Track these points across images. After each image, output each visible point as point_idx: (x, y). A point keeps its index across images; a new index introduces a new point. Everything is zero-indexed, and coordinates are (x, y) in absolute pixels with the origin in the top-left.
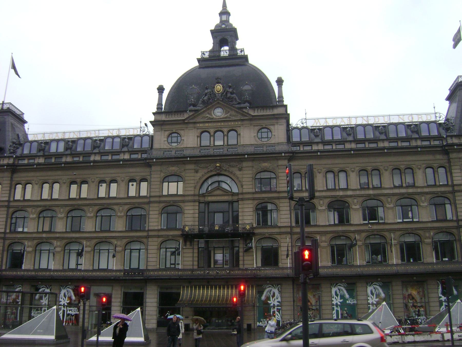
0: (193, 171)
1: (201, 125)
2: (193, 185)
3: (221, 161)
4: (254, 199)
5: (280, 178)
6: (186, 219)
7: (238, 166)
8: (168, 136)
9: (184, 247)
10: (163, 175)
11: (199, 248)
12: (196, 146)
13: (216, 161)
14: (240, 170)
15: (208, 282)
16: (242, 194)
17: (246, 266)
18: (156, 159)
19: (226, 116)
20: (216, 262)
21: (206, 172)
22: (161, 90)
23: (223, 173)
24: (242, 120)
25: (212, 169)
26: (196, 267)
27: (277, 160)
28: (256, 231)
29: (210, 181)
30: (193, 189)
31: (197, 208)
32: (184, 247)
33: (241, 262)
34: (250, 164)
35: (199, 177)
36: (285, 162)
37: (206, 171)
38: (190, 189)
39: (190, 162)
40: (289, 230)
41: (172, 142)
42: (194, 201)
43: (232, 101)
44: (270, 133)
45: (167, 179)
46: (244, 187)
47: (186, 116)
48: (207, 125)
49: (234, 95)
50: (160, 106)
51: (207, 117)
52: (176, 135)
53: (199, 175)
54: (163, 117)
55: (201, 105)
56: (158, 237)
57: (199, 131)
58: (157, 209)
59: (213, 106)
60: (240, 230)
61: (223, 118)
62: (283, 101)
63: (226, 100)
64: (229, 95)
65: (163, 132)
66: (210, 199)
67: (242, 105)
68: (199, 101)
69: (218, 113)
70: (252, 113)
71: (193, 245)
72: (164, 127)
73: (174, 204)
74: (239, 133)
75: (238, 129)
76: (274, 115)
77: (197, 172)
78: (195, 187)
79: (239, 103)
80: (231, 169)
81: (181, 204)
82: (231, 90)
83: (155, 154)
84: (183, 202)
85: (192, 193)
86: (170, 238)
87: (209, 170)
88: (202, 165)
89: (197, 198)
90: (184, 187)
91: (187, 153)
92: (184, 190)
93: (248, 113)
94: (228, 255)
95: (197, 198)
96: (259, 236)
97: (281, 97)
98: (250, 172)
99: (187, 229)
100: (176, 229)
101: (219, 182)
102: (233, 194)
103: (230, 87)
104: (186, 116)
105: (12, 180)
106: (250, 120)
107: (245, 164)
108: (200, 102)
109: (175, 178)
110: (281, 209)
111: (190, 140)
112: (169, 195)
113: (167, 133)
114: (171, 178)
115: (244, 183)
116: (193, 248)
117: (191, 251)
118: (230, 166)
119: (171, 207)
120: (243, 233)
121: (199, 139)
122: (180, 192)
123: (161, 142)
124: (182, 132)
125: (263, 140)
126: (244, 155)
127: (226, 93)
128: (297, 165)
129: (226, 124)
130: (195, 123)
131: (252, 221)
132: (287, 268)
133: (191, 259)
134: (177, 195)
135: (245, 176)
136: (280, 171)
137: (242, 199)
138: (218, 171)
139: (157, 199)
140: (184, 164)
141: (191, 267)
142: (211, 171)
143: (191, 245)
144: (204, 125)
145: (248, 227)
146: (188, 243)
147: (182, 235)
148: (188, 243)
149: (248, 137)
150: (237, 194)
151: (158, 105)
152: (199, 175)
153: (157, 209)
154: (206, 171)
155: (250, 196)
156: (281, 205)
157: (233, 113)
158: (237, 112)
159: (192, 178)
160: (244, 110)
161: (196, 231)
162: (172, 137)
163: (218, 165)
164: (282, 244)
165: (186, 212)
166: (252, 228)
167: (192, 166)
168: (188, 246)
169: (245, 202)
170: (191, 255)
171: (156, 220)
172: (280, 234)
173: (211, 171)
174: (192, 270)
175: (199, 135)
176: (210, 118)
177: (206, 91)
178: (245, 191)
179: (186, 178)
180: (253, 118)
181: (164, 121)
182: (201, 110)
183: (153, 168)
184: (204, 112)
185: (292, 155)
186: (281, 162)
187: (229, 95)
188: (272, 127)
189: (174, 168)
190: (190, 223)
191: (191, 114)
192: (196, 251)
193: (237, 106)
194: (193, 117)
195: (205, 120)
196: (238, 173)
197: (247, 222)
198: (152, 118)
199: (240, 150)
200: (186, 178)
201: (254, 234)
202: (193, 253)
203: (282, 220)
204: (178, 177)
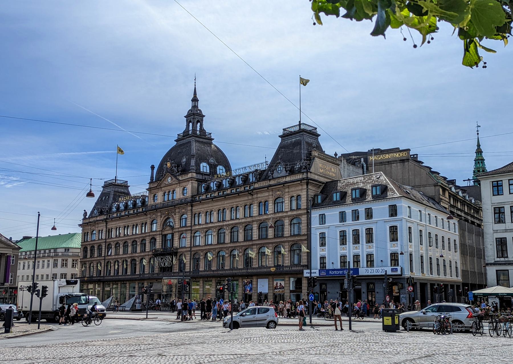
22: (153, 167)
53: (162, 219)
54: (152, 186)
63: (171, 172)
85: (159, 230)
91: (159, 206)
105: (106, 228)
106: (179, 183)
111: (160, 199)
130: (161, 188)
152: (162, 219)
155: (177, 230)
180: (180, 182)
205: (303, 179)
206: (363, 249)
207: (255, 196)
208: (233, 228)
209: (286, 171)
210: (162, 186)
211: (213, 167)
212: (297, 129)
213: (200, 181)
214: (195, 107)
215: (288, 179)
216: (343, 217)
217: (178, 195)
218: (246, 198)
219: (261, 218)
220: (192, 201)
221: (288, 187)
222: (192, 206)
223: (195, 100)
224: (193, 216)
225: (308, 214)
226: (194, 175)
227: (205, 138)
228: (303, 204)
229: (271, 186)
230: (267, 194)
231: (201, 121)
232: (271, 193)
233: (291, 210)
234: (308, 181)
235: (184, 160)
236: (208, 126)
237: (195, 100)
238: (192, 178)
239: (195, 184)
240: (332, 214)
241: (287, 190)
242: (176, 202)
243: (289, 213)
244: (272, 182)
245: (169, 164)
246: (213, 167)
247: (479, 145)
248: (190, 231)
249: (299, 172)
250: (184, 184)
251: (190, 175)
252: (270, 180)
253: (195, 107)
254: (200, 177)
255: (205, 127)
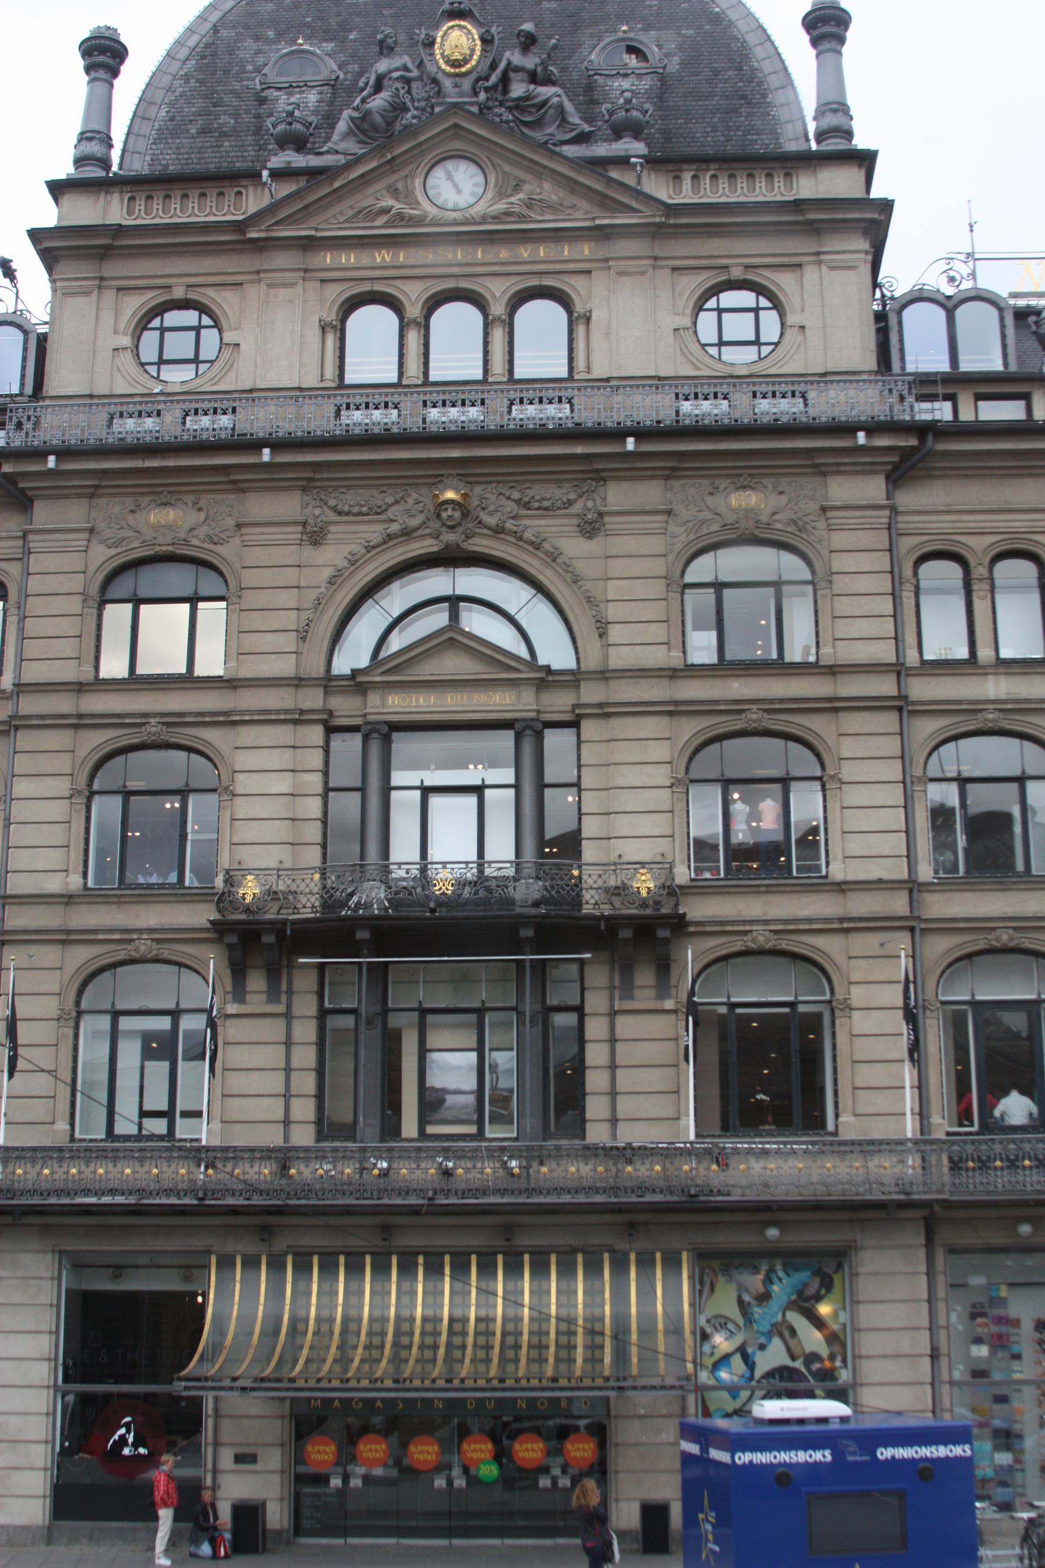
0: (294, 533)
1: (348, 258)
2: (290, 619)
3: (466, 470)
4: (676, 710)
5: (841, 584)
6: (248, 832)
7: (577, 508)
8: (142, 325)
9: (232, 1009)
10: (102, 556)
11: (323, 1014)
12: (311, 380)
13: (437, 471)
14: (590, 528)
15: (384, 1233)
16: (604, 675)
17: (630, 1134)
18: (64, 453)
19: (501, 206)
20: (431, 1103)
21: (376, 538)
22: (104, 54)
23: (481, 545)
24: (602, 234)
25: (414, 523)
26: (304, 1136)
27: (822, 472)
28: (696, 910)
29: (399, 596)
30: (288, 642)
31: (316, 759)
32: (232, 1009)
33: (595, 1107)
34: (650, 493)
35: (327, 573)
36: (873, 488)
37: (374, 532)
38: (269, 641)
39: (272, 479)
40: (898, 904)
41: (161, 362)
42: (298, 719)
43: (538, 124)
44: (770, 320)
45: (124, 585)
46: (616, 633)
47: (254, 201)
48: (383, 257)
49: (546, 91)
50: (95, 148)
51: (386, 211)
52: (190, 317)
54: (112, 211)
55: (353, 147)
56: (67, 938)
57: (336, 293)
58: (64, 763)
59: (421, 150)
60: (592, 903)
61: (484, 219)
62: (849, 134)
63: (503, 115)
64: (518, 89)
65: (110, 295)
66: (398, 704)
67: (601, 150)
68: (330, 120)
69: (456, 189)
71: (290, 992)
72: (114, 268)
73: (167, 736)
74: (579, 308)
75: (575, 286)
76: (798, 205)
77: (316, 537)
78: (303, 635)
79: (583, 138)
80: (534, 526)
81: (213, 736)
82: (530, 62)
83: (56, 426)
84: (228, 720)
85: (285, 667)
86: (143, 946)
87: (394, 528)
88: (351, 499)
89: (312, 699)
90: (234, 633)
91: (257, 420)
92: (234, 651)
93: (638, 194)
94: (505, 1060)
95: (312, 699)
96: (711, 942)
97: (834, 107)
98: (655, 544)
99: (250, 889)
100: (178, 893)
101: (454, 602)
102: (547, 679)
103: (528, 42)
104: (254, 201)
106: (655, 232)
107: (617, 495)
108: (342, 126)
109: (179, 578)
110: (847, 772)
111: (273, 347)
112: (136, 681)
113: (134, 305)
114: (150, 580)
115: (613, 612)
116: (288, 1016)
117: (275, 1029)
118: (527, 506)
120: (613, 923)
121: (331, 341)
122: (211, 662)
124: (225, 301)
125: (730, 354)
126: (619, 434)
127: (505, 80)
129: (504, 253)
130: (309, 244)
131: (664, 845)
132: (895, 1146)
133: (275, 1083)
134: (188, 681)
135: (617, 567)
136: (839, 539)
137: (605, 712)
138: (449, 537)
139: (63, 704)
140: (239, 488)
141: (273, 1137)
142: (407, 534)
143: (273, 993)
144: (365, 261)
145: (645, 883)
146: (257, 982)
147: (220, 929)
148: (257, 982)
149: (636, 335)
150: (573, 679)
151: (84, 137)
152: (331, 556)
153: (64, 763)
154: (374, 532)
156: (848, 748)
157: (548, 191)
158: (572, 186)
159: (290, 576)
160: (614, 174)
161: (308, 906)
162: (163, 330)
163: (450, 495)
164: (855, 990)
165: (243, 783)
166: (672, 891)
167: (288, 505)
168: (257, 1001)
169: (622, 727)
170: (275, 1056)
171: (56, 835)
172: (846, 927)
173: (407, 534)
174: (284, 1157)
175: (332, 317)
176: (400, 216)
177: (383, 66)
178: (619, 658)
179: (249, 578)
180: (673, 224)
181: (119, 230)
182: (348, 166)
183: (43, 513)
184: (365, 180)
185: (913, 442)
186: (842, 489)
187: (518, 89)
188: (784, 282)
189: (171, 515)
190: (269, 858)
191: (286, 189)
192: (306, 1031)
193: (571, 151)
195: (378, 227)
196: (575, 547)
197: (633, 851)
198: (47, 214)
199: (591, 410)
200: (246, 574)
201: (679, 925)
202: (288, 1043)
203: (855, 845)
204: (193, 570)
210: (331, 223)
222: (902, 470)
224: (908, 572)
248: (889, 721)
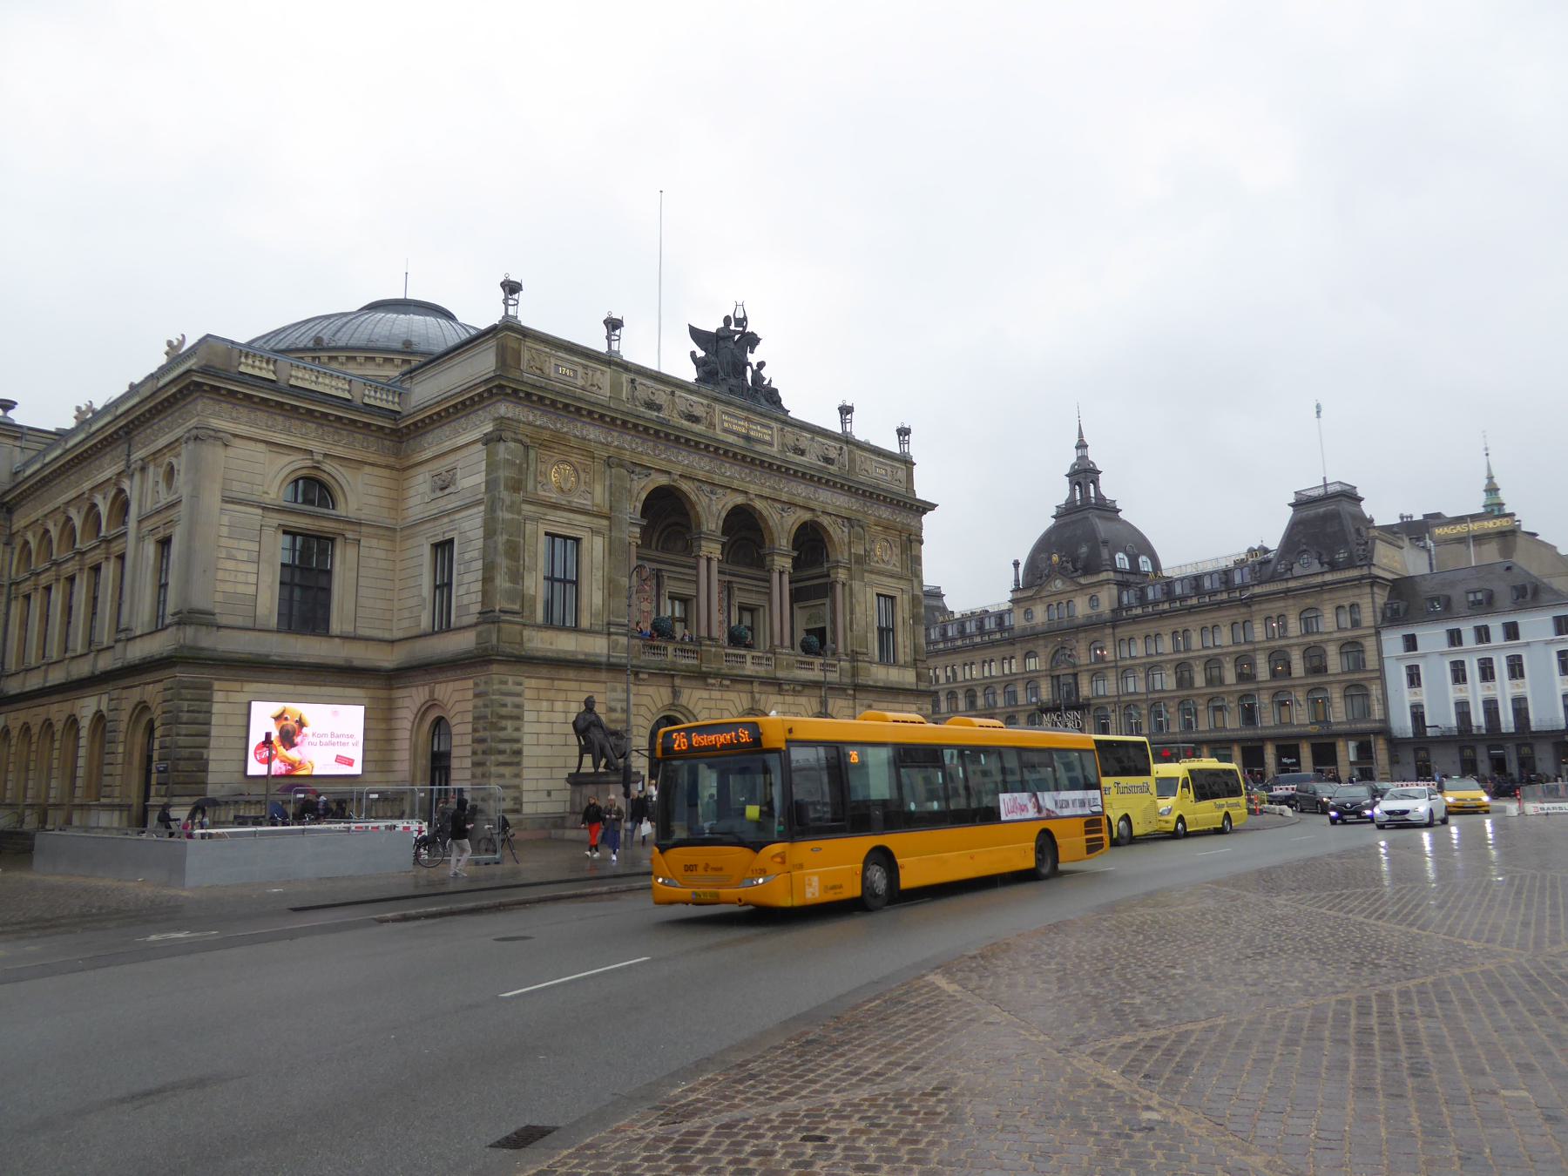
22: (1016, 564)
54: (1019, 595)
63: (1061, 571)
69: (1059, 584)
70: (1083, 581)
91: (1039, 629)
111: (1040, 615)
119: (1031, 682)
123: (1017, 621)
128: (1122, 632)
167: (1041, 642)
180: (1083, 587)
194: (1038, 592)
204: (1029, 654)
205: (1363, 577)
206: (1504, 690)
207: (1254, 608)
208: (1212, 663)
209: (1322, 564)
211: (1134, 560)
212: (1321, 491)
213: (1123, 585)
214: (1083, 458)
215: (1328, 577)
216: (1455, 638)
217: (1081, 608)
218: (1234, 611)
219: (1273, 644)
220: (1117, 619)
221: (1331, 591)
222: (1114, 628)
223: (1082, 445)
225: (1378, 634)
226: (1111, 575)
227: (1108, 510)
228: (1367, 617)
229: (1288, 590)
230: (1281, 604)
231: (1095, 482)
232: (1291, 602)
233: (1339, 629)
234: (1374, 581)
235: (1084, 550)
236: (1109, 487)
237: (1082, 445)
238: (1108, 582)
239: (1114, 590)
240: (1432, 637)
241: (1326, 596)
242: (1081, 621)
243: (1336, 635)
244: (1292, 584)
245: (1055, 558)
246: (1134, 560)
247: (1490, 478)
249: (1349, 564)
250: (1092, 591)
251: (1103, 576)
252: (1287, 580)
253: (1083, 458)
254: (1119, 577)
255: (1104, 491)
